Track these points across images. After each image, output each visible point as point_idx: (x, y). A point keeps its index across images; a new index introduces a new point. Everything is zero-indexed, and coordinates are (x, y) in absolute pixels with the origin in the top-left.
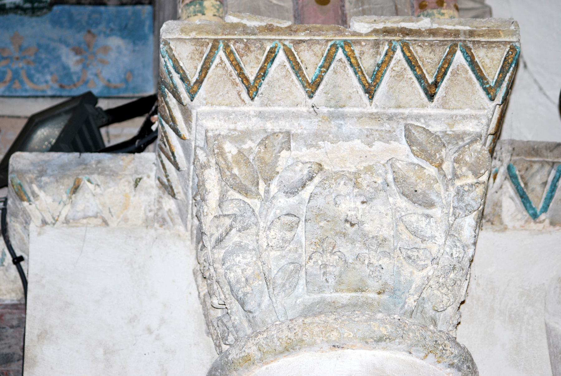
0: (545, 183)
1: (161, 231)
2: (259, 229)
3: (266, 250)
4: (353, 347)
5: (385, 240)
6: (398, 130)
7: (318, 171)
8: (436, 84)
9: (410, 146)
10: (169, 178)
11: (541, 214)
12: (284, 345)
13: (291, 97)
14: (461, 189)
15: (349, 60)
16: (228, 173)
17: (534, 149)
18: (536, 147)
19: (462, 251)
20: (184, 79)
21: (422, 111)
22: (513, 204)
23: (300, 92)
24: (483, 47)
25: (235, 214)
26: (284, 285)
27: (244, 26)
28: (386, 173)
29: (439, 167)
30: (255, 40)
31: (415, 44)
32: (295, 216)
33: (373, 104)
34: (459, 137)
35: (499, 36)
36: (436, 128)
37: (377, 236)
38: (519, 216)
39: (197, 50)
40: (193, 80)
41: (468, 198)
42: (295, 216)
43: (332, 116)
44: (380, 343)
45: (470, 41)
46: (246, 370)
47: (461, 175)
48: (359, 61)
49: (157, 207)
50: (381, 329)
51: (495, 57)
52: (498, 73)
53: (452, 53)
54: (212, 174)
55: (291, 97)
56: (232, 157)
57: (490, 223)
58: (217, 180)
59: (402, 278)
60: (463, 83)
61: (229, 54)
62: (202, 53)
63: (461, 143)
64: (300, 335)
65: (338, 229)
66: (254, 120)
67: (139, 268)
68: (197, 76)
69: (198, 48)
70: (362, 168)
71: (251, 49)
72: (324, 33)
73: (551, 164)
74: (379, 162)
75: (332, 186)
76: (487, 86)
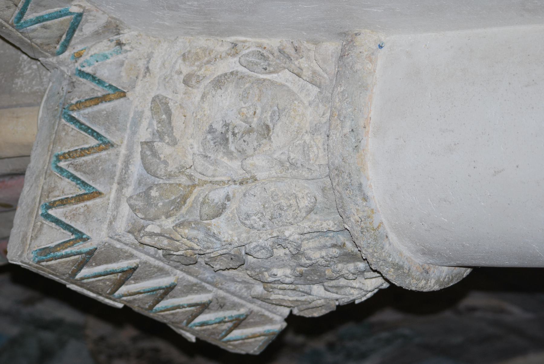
0: (45, 27)
62: (241, 344)
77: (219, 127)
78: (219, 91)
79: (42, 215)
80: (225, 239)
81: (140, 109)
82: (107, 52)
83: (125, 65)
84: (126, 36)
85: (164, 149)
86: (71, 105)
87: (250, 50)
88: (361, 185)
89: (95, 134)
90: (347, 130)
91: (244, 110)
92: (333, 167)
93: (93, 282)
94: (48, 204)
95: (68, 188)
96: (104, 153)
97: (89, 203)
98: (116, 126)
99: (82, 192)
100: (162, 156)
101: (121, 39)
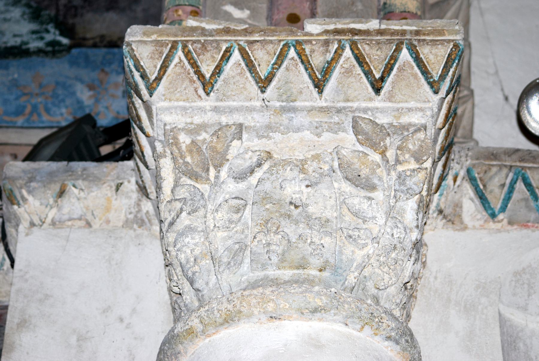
0: (503, 185)
1: (139, 231)
2: (207, 211)
3: (213, 230)
4: (289, 318)
5: (328, 221)
6: (347, 122)
7: (267, 159)
8: (382, 79)
9: (356, 135)
10: (143, 179)
11: (499, 214)
12: (224, 316)
13: (245, 93)
14: (403, 174)
15: (300, 58)
16: (181, 161)
17: (493, 154)
18: (495, 152)
19: (403, 231)
20: (144, 76)
21: (370, 105)
22: (473, 205)
23: (253, 88)
24: (427, 44)
25: (185, 198)
26: (229, 263)
27: (203, 29)
28: (333, 161)
29: (383, 153)
30: (212, 41)
31: (363, 42)
32: (242, 199)
33: (323, 98)
34: (404, 128)
35: (444, 35)
36: (383, 120)
37: (320, 218)
38: (479, 216)
39: (157, 50)
40: (153, 78)
41: (410, 183)
42: (242, 199)
43: (283, 110)
44: (315, 314)
45: (416, 40)
46: (191, 343)
47: (403, 161)
48: (310, 58)
49: (137, 209)
50: (316, 300)
51: (439, 54)
52: (441, 68)
53: (398, 50)
54: (168, 163)
55: (245, 93)
56: (186, 147)
57: (451, 223)
58: (172, 169)
59: (344, 256)
60: (409, 78)
61: (187, 54)
62: (161, 53)
63: (406, 133)
64: (238, 306)
65: (283, 211)
66: (209, 114)
67: (117, 264)
68: (156, 74)
69: (157, 48)
70: (310, 156)
71: (208, 49)
72: (277, 34)
73: (509, 167)
74: (326, 151)
75: (279, 172)
76: (431, 80)
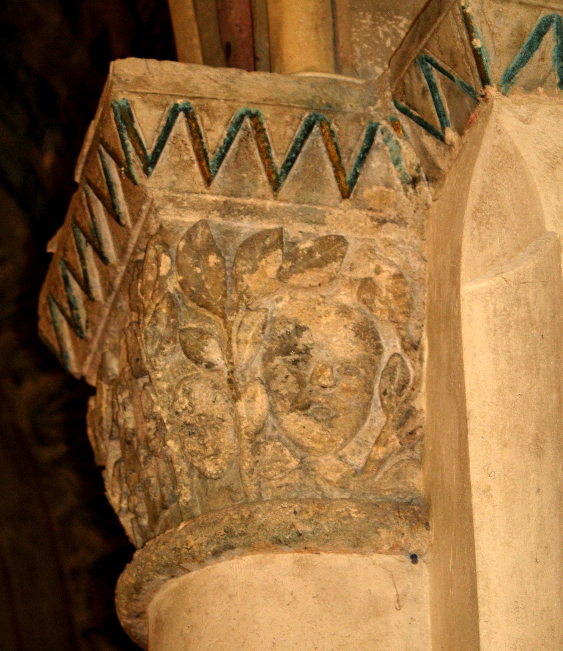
0: (424, 92)
77: (304, 340)
78: (353, 334)
79: (177, 105)
80: (158, 362)
81: (328, 219)
82: (403, 163)
83: (387, 190)
84: (426, 189)
85: (272, 264)
86: (329, 124)
87: (411, 368)
88: (232, 548)
89: (290, 164)
90: (300, 527)
91: (328, 373)
92: (253, 510)
93: (98, 165)
94: (191, 111)
95: (215, 136)
96: (264, 177)
97: (196, 167)
98: (302, 189)
99: (211, 156)
100: (263, 262)
101: (422, 182)
